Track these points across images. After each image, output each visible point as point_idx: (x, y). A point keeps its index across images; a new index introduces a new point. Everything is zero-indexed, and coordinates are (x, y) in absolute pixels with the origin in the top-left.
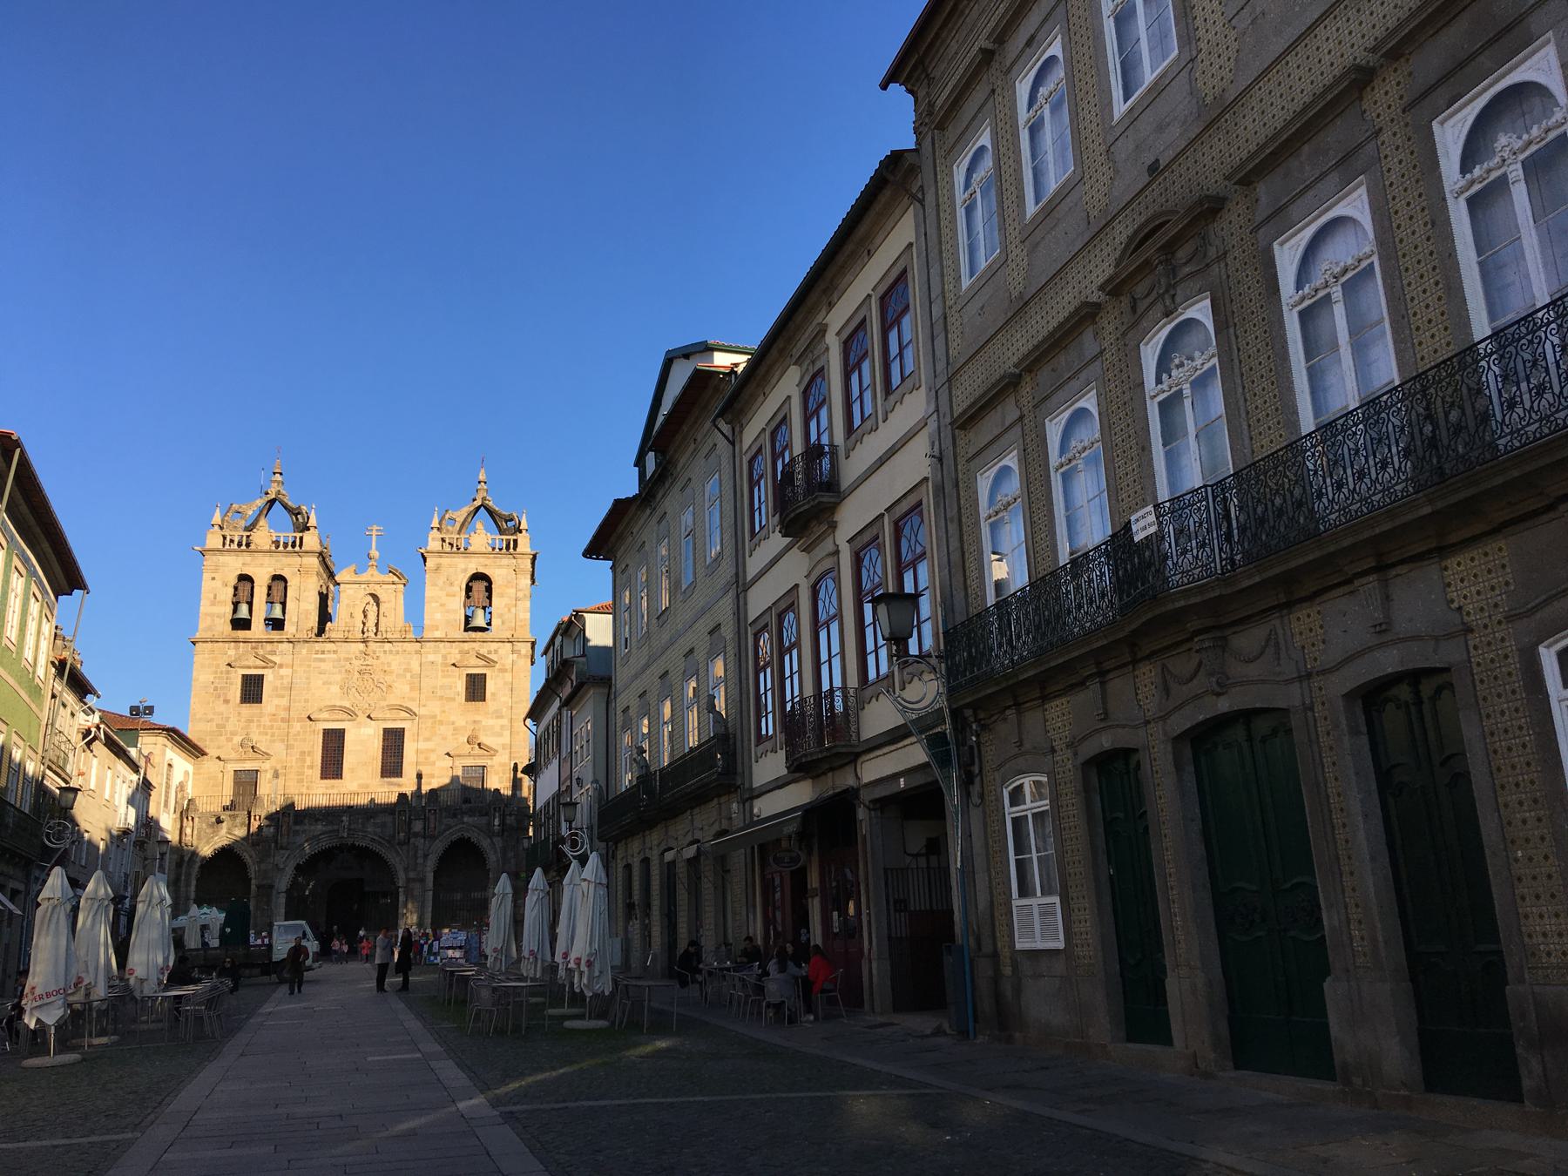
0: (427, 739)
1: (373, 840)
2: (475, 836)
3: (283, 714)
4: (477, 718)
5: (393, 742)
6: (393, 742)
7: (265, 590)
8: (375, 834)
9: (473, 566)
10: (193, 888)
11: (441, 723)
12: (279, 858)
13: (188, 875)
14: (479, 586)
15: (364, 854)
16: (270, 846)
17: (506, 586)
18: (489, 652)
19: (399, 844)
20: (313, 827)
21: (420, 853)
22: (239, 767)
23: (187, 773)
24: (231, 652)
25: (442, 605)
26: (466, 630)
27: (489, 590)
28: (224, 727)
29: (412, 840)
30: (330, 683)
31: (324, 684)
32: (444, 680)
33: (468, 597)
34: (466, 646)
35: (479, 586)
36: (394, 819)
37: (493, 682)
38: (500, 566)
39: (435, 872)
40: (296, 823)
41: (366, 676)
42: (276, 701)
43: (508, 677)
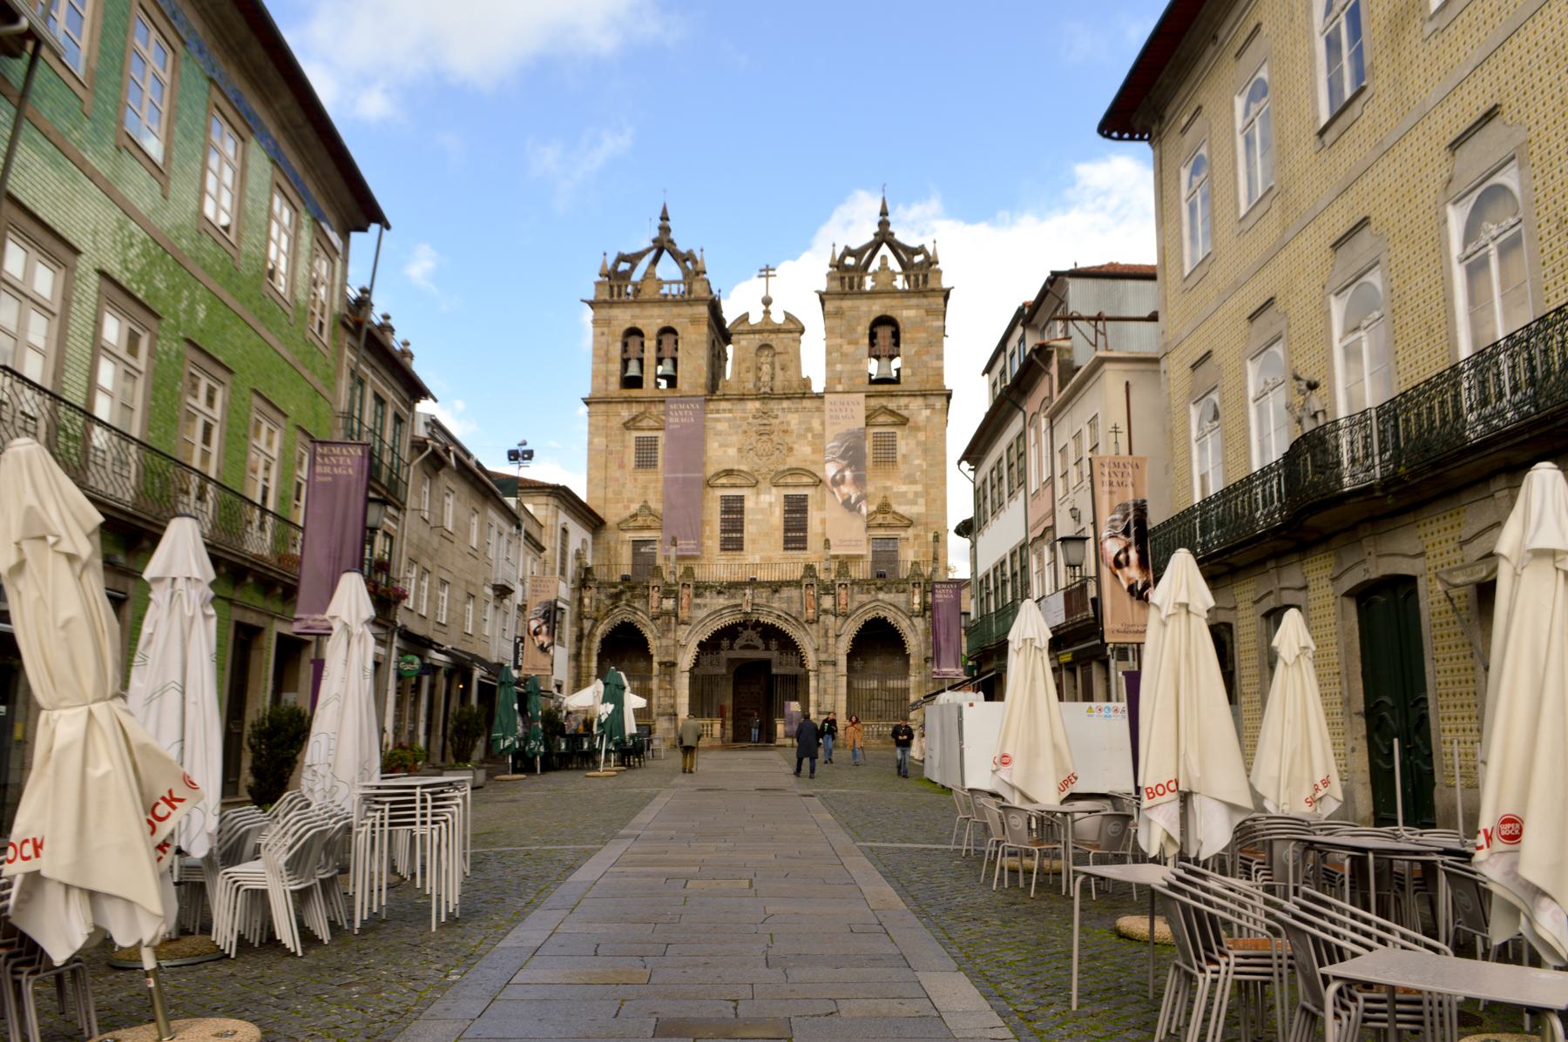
1: (779, 617)
4: (889, 484)
5: (796, 510)
6: (796, 510)
7: (654, 343)
9: (877, 308)
12: (683, 631)
13: (589, 649)
14: (884, 333)
15: (771, 634)
18: (899, 407)
19: (807, 621)
20: (715, 601)
21: (831, 633)
23: (584, 541)
24: (625, 413)
27: (896, 335)
28: (620, 493)
29: (822, 618)
30: (726, 446)
31: (720, 446)
33: (872, 344)
35: (884, 333)
39: (848, 655)
40: (697, 596)
43: (921, 436)
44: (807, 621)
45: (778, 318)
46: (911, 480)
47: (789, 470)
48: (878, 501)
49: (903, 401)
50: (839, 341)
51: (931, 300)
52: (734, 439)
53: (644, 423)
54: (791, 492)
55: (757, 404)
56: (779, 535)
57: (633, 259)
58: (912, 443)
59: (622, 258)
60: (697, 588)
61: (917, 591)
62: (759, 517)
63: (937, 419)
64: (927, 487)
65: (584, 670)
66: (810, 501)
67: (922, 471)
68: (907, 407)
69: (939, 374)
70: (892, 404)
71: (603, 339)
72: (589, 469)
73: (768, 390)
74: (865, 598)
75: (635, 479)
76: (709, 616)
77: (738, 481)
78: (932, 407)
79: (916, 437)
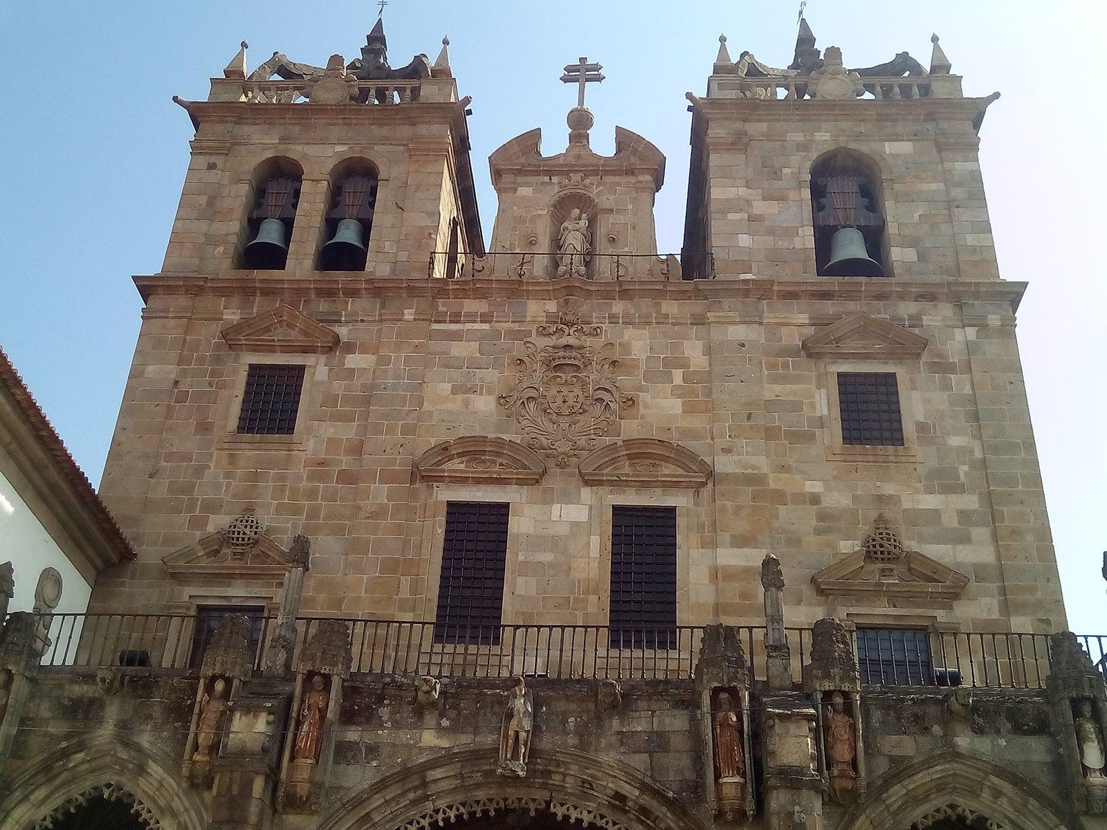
0: (741, 541)
3: (345, 461)
4: (889, 489)
8: (631, 777)
11: (779, 497)
16: (247, 786)
17: (917, 177)
20: (405, 736)
22: (213, 594)
23: (50, 578)
25: (752, 219)
27: (870, 195)
28: (189, 488)
31: (454, 391)
32: (778, 388)
34: (829, 307)
36: (695, 722)
37: (916, 395)
38: (896, 138)
42: (328, 430)
43: (961, 384)
44: (719, 815)
46: (945, 482)
47: (628, 443)
48: (864, 529)
50: (743, 191)
51: (944, 125)
52: (491, 375)
53: (277, 335)
54: (631, 499)
55: (552, 307)
56: (598, 607)
58: (940, 400)
60: (351, 691)
62: (547, 557)
63: (992, 347)
64: (989, 498)
67: (973, 464)
68: (916, 321)
69: (987, 258)
70: (882, 313)
71: (212, 176)
72: (120, 429)
74: (906, 745)
75: (233, 459)
76: (380, 786)
78: (983, 327)
79: (947, 387)
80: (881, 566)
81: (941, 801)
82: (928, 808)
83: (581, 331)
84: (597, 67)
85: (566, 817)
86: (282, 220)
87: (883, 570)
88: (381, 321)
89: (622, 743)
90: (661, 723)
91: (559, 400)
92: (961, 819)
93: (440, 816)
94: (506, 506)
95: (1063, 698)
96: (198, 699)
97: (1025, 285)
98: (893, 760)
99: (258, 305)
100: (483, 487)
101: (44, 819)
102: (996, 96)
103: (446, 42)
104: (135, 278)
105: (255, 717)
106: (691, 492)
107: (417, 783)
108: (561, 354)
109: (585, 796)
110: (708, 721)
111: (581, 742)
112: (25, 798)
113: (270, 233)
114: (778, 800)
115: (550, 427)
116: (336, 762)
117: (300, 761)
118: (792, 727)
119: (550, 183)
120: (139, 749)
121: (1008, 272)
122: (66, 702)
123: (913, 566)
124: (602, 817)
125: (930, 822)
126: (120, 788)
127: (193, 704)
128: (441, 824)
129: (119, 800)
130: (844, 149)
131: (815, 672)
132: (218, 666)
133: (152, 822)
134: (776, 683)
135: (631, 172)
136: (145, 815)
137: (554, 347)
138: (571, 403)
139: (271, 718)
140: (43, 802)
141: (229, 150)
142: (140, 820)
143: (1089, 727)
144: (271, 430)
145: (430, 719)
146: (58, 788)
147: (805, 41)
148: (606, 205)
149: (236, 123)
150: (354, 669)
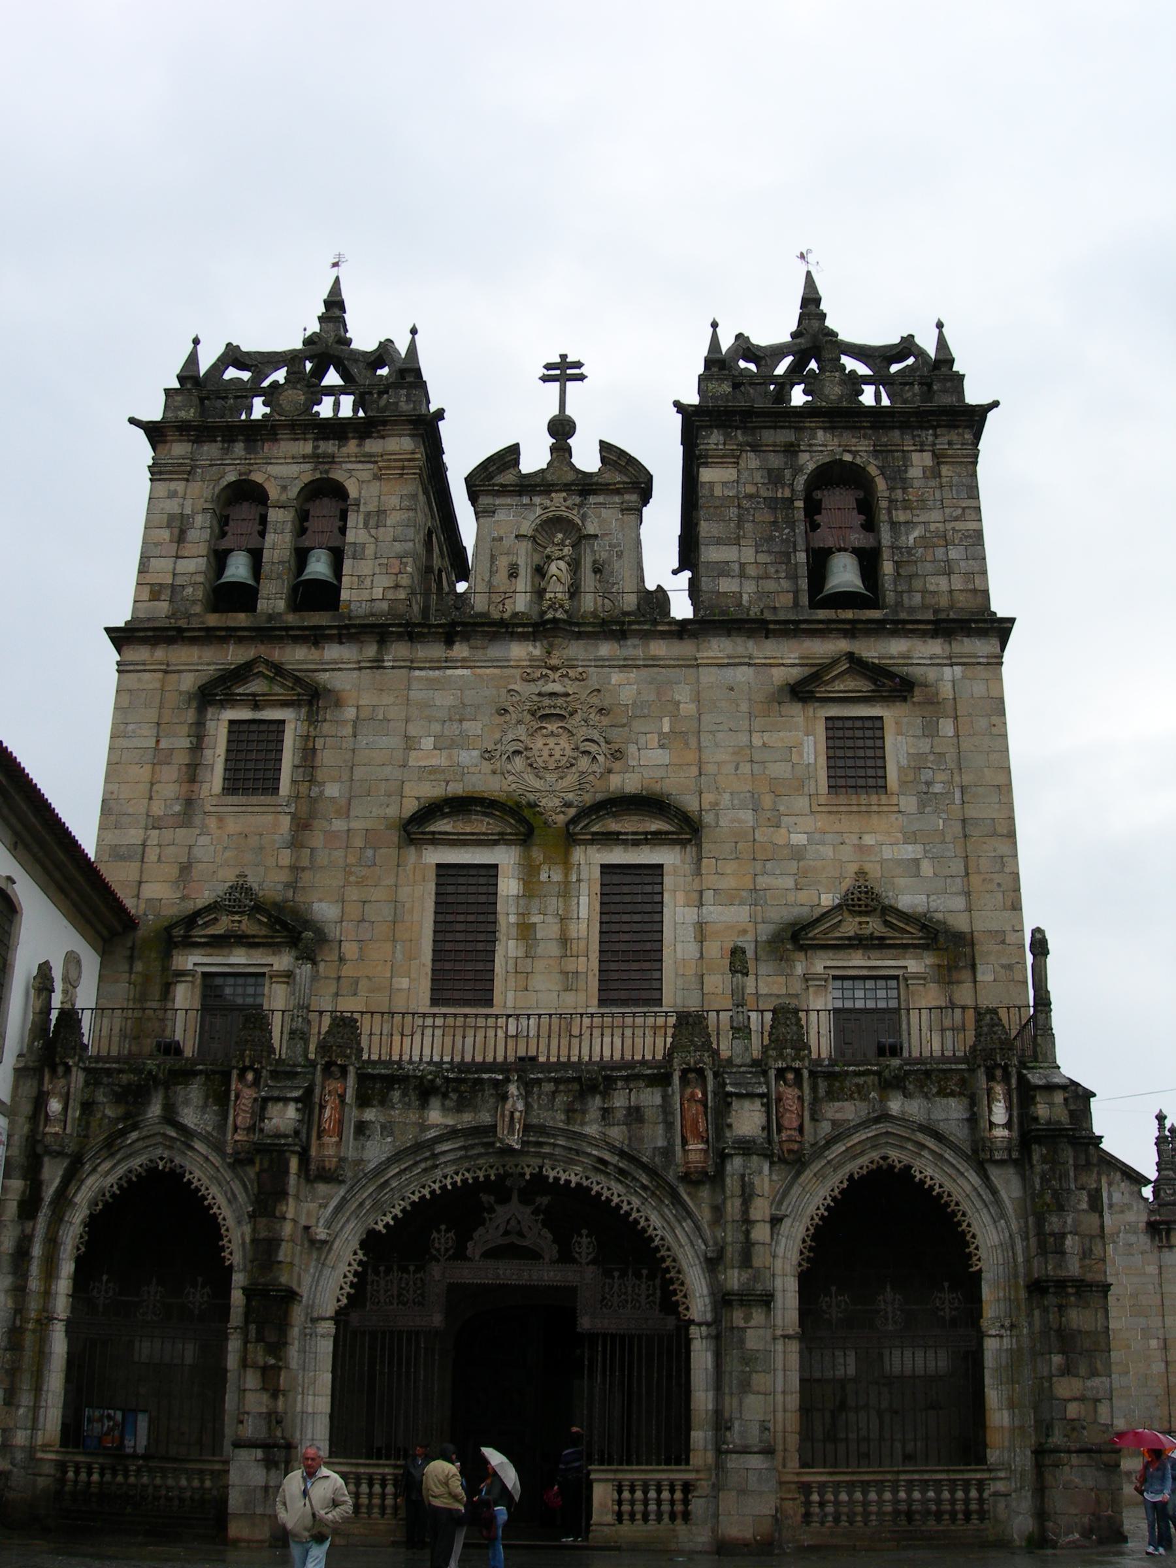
2: (927, 1170)
8: (612, 1149)
10: (63, 1286)
19: (686, 1178)
20: (413, 1117)
21: (761, 1209)
23: (72, 960)
26: (814, 605)
27: (867, 508)
41: (552, 727)
45: (586, 459)
48: (847, 884)
49: (896, 647)
54: (618, 856)
55: (537, 651)
57: (260, 363)
59: (233, 356)
60: (362, 1078)
61: (999, 1089)
65: (33, 1306)
66: (667, 880)
70: (872, 650)
73: (560, 615)
77: (481, 825)
80: (858, 919)
81: (875, 1155)
82: (864, 1160)
83: (567, 676)
84: (579, 365)
85: (557, 1179)
86: (249, 551)
87: (860, 923)
88: (360, 669)
89: (603, 1118)
90: (638, 1098)
91: (546, 753)
92: (891, 1167)
93: (449, 1181)
94: (496, 866)
95: (979, 1066)
96: (233, 1087)
97: (1012, 621)
98: (834, 1123)
99: (235, 655)
100: (471, 849)
101: (112, 1186)
102: (996, 404)
103: (414, 331)
104: (108, 630)
105: (286, 1105)
106: (678, 848)
107: (428, 1154)
108: (547, 702)
109: (572, 1162)
110: (677, 1098)
111: (568, 1118)
112: (94, 1170)
113: (238, 569)
114: (736, 1164)
115: (538, 784)
116: (355, 1139)
117: (326, 1139)
118: (747, 1104)
119: (533, 505)
120: (182, 1129)
121: (1000, 607)
122: (116, 1088)
123: (889, 918)
124: (587, 1178)
125: (865, 1172)
126: (172, 1161)
127: (228, 1091)
128: (449, 1187)
129: (172, 1170)
130: (841, 460)
131: (771, 1052)
132: (247, 1060)
133: (203, 1189)
134: (738, 1061)
135: (618, 492)
136: (196, 1183)
137: (540, 694)
138: (557, 756)
139: (300, 1105)
140: (108, 1173)
141: (189, 473)
142: (193, 1186)
143: (999, 1089)
144: (255, 791)
145: (435, 1102)
146: (119, 1162)
147: (811, 302)
148: (591, 529)
149: (194, 442)
150: (365, 1057)
